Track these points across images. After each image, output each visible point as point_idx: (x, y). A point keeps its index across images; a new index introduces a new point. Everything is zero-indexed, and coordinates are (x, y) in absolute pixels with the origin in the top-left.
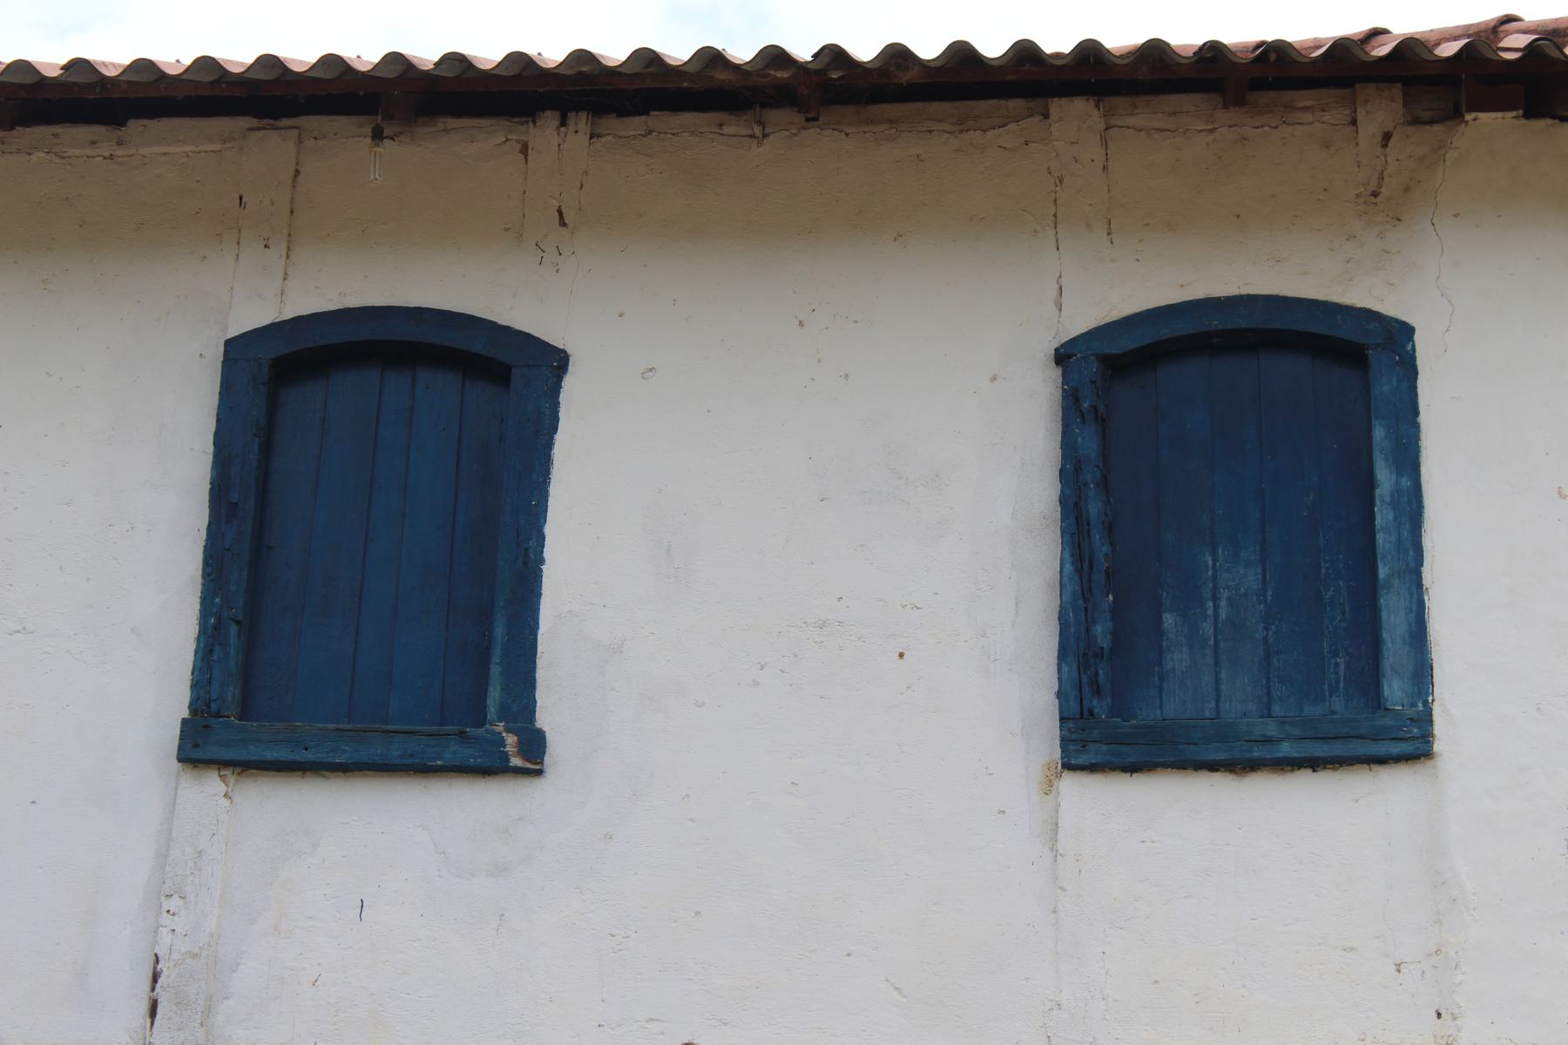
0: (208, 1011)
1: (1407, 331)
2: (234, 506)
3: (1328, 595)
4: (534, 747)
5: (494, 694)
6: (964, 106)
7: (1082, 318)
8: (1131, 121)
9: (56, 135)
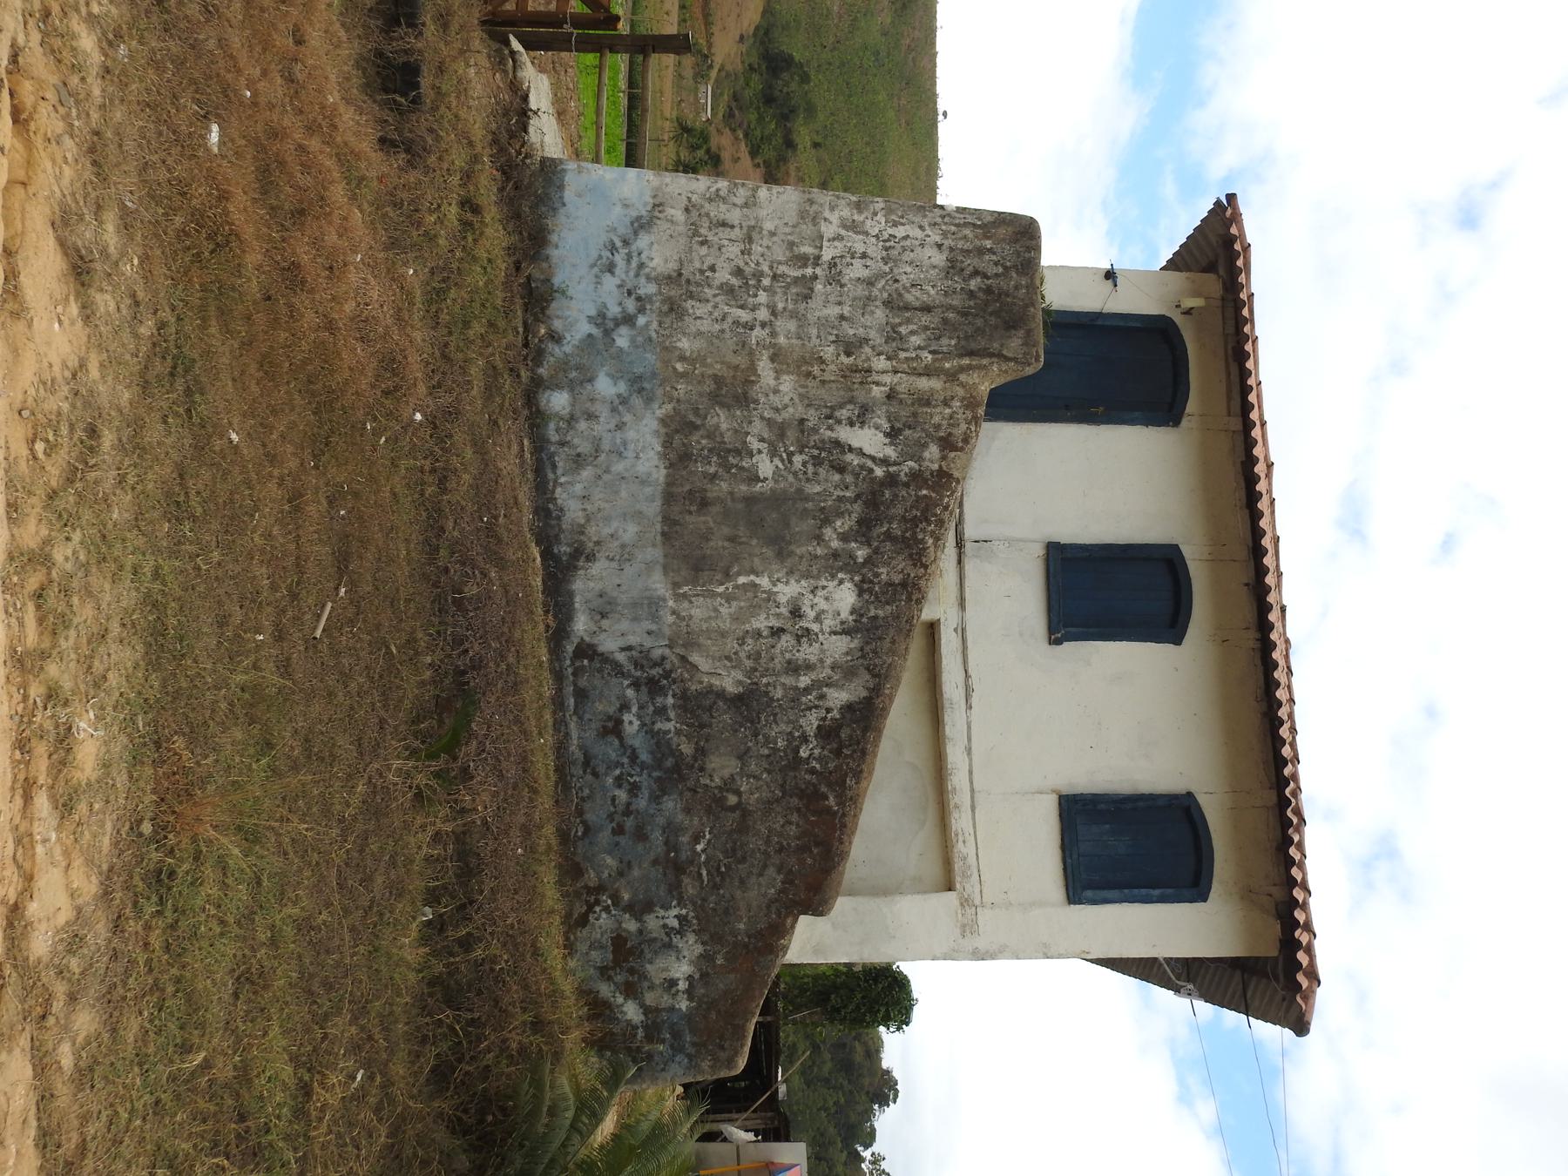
0: (976, 557)
1: (1205, 900)
4: (1058, 642)
7: (1203, 800)
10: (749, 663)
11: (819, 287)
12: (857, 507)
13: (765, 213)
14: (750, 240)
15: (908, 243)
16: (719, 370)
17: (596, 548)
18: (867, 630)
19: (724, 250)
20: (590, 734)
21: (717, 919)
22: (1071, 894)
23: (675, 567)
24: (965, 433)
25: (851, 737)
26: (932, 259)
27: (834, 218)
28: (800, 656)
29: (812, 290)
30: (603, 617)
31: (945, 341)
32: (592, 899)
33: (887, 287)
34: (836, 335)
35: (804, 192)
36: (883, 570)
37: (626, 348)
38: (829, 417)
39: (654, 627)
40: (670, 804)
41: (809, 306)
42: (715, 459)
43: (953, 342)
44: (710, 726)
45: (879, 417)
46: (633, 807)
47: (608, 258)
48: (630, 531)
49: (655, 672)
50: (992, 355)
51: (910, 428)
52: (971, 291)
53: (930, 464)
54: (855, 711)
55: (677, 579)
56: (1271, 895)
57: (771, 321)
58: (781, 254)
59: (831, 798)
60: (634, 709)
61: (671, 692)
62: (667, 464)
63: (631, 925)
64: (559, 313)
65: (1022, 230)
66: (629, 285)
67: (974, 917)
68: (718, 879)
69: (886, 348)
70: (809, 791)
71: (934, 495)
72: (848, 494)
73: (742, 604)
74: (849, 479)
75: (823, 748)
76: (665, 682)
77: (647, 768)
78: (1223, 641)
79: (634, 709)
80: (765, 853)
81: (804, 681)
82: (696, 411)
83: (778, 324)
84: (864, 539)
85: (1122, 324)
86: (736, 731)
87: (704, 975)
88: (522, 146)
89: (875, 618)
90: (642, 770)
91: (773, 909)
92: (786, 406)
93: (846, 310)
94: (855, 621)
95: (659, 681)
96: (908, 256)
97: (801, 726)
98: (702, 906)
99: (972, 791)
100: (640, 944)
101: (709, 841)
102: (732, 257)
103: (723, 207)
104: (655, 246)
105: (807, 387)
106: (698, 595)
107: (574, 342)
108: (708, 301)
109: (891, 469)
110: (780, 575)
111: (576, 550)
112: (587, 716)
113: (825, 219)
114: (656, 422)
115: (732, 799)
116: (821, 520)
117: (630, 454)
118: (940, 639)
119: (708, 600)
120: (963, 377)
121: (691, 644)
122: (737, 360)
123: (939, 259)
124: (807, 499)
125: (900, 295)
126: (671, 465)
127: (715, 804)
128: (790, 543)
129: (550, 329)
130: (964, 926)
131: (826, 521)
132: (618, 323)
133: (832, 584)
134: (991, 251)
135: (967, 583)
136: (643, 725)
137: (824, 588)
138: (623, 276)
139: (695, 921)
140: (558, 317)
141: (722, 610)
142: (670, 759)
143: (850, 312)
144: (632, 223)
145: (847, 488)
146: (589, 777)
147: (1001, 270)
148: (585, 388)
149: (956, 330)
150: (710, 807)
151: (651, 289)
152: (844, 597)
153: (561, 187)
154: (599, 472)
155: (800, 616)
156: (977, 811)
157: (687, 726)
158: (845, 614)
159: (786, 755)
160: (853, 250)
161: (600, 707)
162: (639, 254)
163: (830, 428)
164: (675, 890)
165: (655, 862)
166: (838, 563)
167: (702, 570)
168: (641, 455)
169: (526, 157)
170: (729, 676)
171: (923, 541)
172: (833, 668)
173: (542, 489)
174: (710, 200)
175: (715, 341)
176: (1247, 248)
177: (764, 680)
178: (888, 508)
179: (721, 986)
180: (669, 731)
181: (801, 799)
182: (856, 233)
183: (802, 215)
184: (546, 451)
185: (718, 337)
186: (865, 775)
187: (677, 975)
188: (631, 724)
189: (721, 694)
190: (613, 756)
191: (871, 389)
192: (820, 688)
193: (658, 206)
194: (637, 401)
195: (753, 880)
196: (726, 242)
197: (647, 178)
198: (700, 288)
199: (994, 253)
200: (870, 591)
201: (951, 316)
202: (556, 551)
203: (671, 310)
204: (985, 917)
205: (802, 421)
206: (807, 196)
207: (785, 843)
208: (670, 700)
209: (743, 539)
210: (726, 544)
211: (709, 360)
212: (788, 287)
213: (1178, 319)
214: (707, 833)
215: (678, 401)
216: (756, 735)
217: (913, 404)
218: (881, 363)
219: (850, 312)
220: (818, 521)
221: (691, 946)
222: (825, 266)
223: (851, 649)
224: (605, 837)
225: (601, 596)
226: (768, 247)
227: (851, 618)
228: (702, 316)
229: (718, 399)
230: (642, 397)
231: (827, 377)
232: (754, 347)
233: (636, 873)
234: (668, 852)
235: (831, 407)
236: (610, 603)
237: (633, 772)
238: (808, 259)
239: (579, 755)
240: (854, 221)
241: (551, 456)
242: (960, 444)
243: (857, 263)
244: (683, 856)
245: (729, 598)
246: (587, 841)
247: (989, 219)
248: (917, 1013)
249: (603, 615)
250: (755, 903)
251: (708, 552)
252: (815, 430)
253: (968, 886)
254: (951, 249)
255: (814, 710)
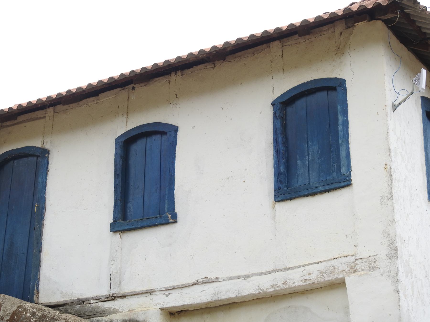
0: (120, 284)
1: (344, 81)
3: (332, 149)
4: (175, 217)
6: (254, 49)
7: (277, 94)
8: (289, 43)
9: (87, 101)
22: (343, 184)
56: (341, 33)
99: (275, 271)
118: (176, 307)
156: (289, 266)
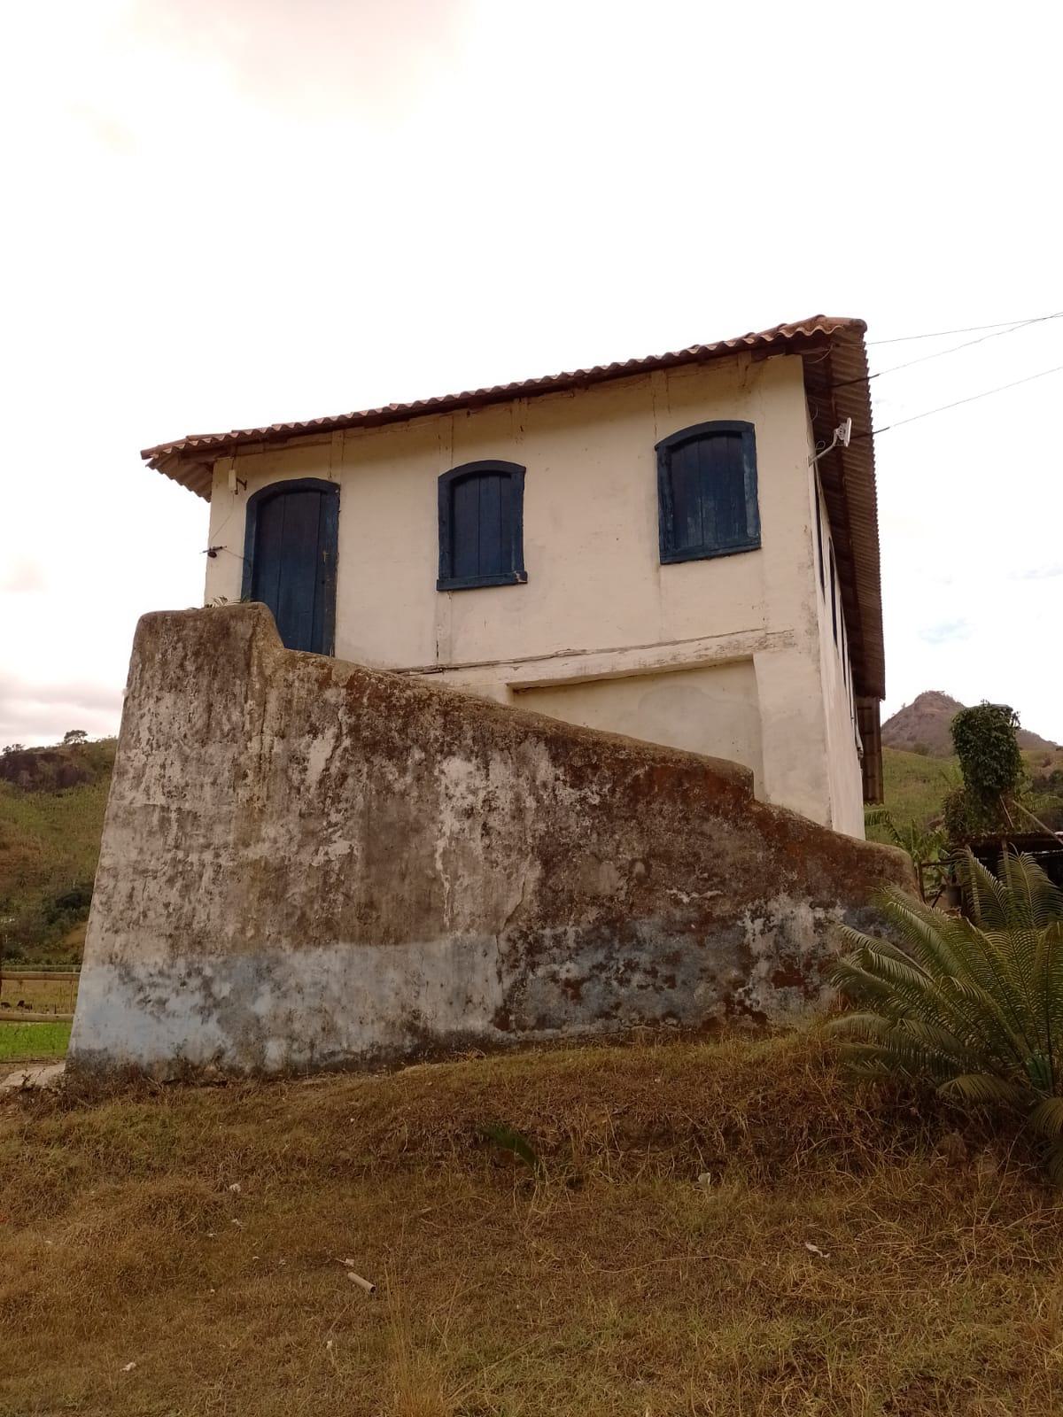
0: (451, 653)
1: (753, 425)
2: (444, 522)
4: (524, 576)
5: (513, 564)
7: (661, 437)
10: (514, 856)
11: (187, 806)
12: (377, 760)
13: (123, 859)
14: (146, 871)
15: (154, 728)
16: (255, 895)
17: (408, 1010)
18: (485, 745)
19: (151, 896)
20: (580, 1012)
21: (754, 880)
22: (751, 547)
23: (426, 930)
24: (317, 667)
25: (581, 756)
26: (169, 705)
27: (130, 795)
28: (507, 807)
29: (189, 812)
30: (470, 1001)
31: (237, 690)
32: (738, 1008)
33: (190, 744)
34: (228, 788)
35: (107, 824)
36: (432, 734)
37: (231, 985)
38: (299, 790)
39: (480, 950)
40: (645, 929)
41: (202, 814)
42: (331, 895)
43: (238, 682)
44: (571, 891)
45: (300, 745)
46: (649, 967)
47: (153, 1006)
48: (393, 976)
49: (521, 947)
50: (250, 647)
51: (309, 717)
52: (196, 669)
53: (341, 697)
54: (558, 753)
55: (438, 928)
56: (747, 367)
57: (214, 849)
58: (158, 843)
59: (638, 772)
60: (556, 967)
61: (540, 931)
62: (333, 942)
63: (763, 967)
64: (198, 1052)
65: (148, 628)
66: (177, 984)
67: (777, 635)
68: (716, 880)
69: (241, 741)
70: (632, 794)
71: (368, 692)
72: (366, 770)
73: (461, 864)
74: (352, 769)
75: (591, 782)
76: (530, 937)
77: (611, 953)
78: (521, 431)
79: (556, 967)
80: (689, 834)
81: (530, 803)
82: (289, 915)
83: (217, 842)
84: (405, 753)
85: (253, 540)
86: (576, 866)
87: (809, 891)
88: (50, 1091)
89: (474, 738)
90: (613, 958)
91: (742, 824)
92: (288, 831)
93: (208, 780)
94: (477, 757)
95: (530, 943)
96: (165, 727)
97: (571, 804)
98: (742, 895)
99: (659, 644)
100: (781, 958)
101: (679, 889)
102: (158, 887)
103: (116, 898)
104: (144, 960)
105: (272, 812)
106: (452, 908)
107: (223, 1038)
108: (194, 909)
109: (345, 731)
110: (435, 830)
111: (409, 1029)
112: (563, 1016)
113: (131, 803)
114: (297, 954)
115: (639, 867)
116: (387, 793)
117: (324, 978)
118: (525, 683)
119: (457, 897)
120: (268, 672)
121: (496, 913)
122: (246, 878)
123: (169, 698)
124: (369, 808)
125: (197, 732)
126: (336, 938)
127: (645, 884)
128: (407, 822)
129: (211, 1061)
130: (787, 645)
131: (388, 789)
132: (210, 995)
133: (444, 781)
134: (163, 655)
135: (474, 661)
136: (570, 958)
137: (447, 788)
138: (169, 990)
139: (757, 902)
140: (201, 1053)
141: (465, 884)
142: (603, 930)
143: (209, 777)
144: (125, 983)
145: (360, 771)
146: (620, 1013)
147: (180, 644)
148: (265, 1025)
149: (228, 680)
150: (646, 889)
151: (181, 962)
152: (456, 768)
153: (91, 1053)
154: (339, 1008)
155: (472, 809)
156: (678, 640)
157: (571, 914)
158: (471, 767)
159: (598, 817)
160: (158, 777)
161: (554, 1003)
162: (151, 975)
163: (308, 789)
164: (726, 923)
165: (701, 944)
166: (425, 775)
167: (430, 904)
168: (325, 967)
169: (59, 1087)
170: (525, 875)
171: (408, 700)
172: (519, 776)
173: (350, 1066)
174: (110, 910)
175: (229, 901)
176: (189, 438)
177: (530, 840)
178: (378, 732)
179: (819, 874)
180: (576, 932)
181: (638, 801)
182: (143, 775)
183: (126, 824)
184: (319, 1063)
185: (225, 898)
186: (618, 742)
187: (811, 919)
188: (569, 970)
189: (542, 882)
190: (599, 988)
191: (276, 754)
192: (537, 788)
193: (111, 959)
194: (278, 973)
195: (715, 845)
196: (146, 894)
197: (87, 971)
198: (183, 917)
199: (166, 651)
200: (450, 745)
201: (216, 686)
202: (409, 1050)
203: (200, 943)
204: (776, 626)
205: (301, 815)
206: (110, 821)
207: (680, 815)
208: (548, 932)
209: (403, 866)
210: (407, 881)
211: (246, 905)
212: (185, 834)
213: (251, 492)
214: (672, 892)
215: (279, 933)
216: (580, 846)
217: (290, 715)
218: (254, 746)
219: (209, 777)
220: (388, 796)
221: (781, 905)
222: (170, 801)
223: (502, 760)
224: (677, 996)
225: (451, 1003)
226: (152, 854)
227: (474, 761)
228: (206, 912)
229: (279, 895)
230: (274, 968)
231: (264, 794)
232: (236, 863)
233: (711, 963)
234: (691, 930)
235: (290, 789)
236: (458, 994)
237: (615, 967)
238: (163, 817)
239: (600, 1023)
240: (134, 778)
241: (323, 1057)
242: (326, 671)
243: (169, 772)
244: (695, 915)
245: (456, 877)
246: (681, 1014)
247: (138, 658)
248: (997, 700)
249: (469, 1001)
250: (737, 843)
251: (413, 899)
252: (309, 803)
253: (748, 643)
254: (161, 689)
255: (556, 792)
